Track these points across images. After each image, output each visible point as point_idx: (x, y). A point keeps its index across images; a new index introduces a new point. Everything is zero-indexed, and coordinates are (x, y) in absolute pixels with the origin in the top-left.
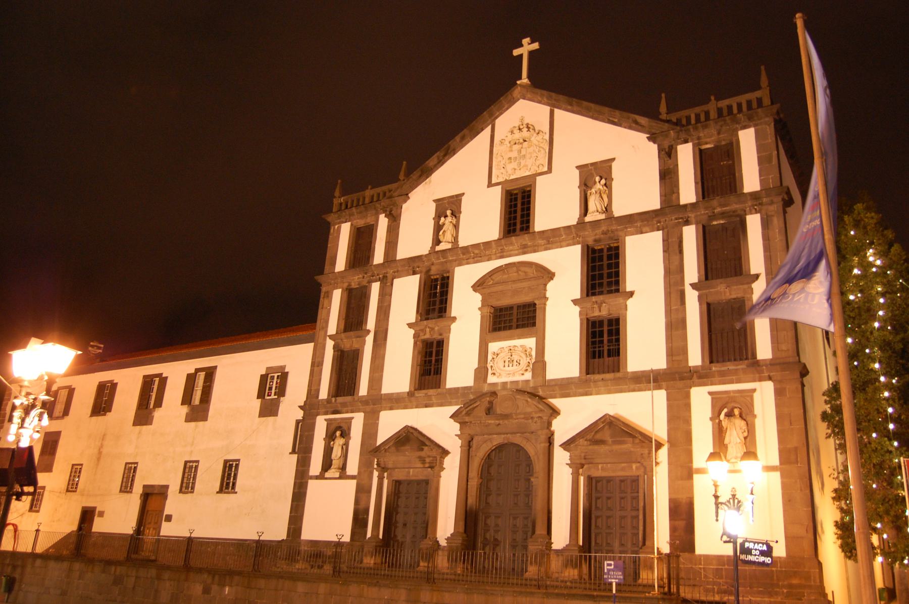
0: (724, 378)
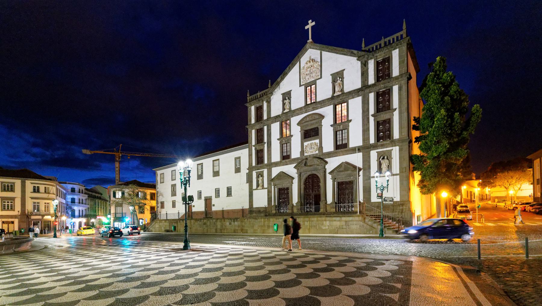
0: (383, 146)
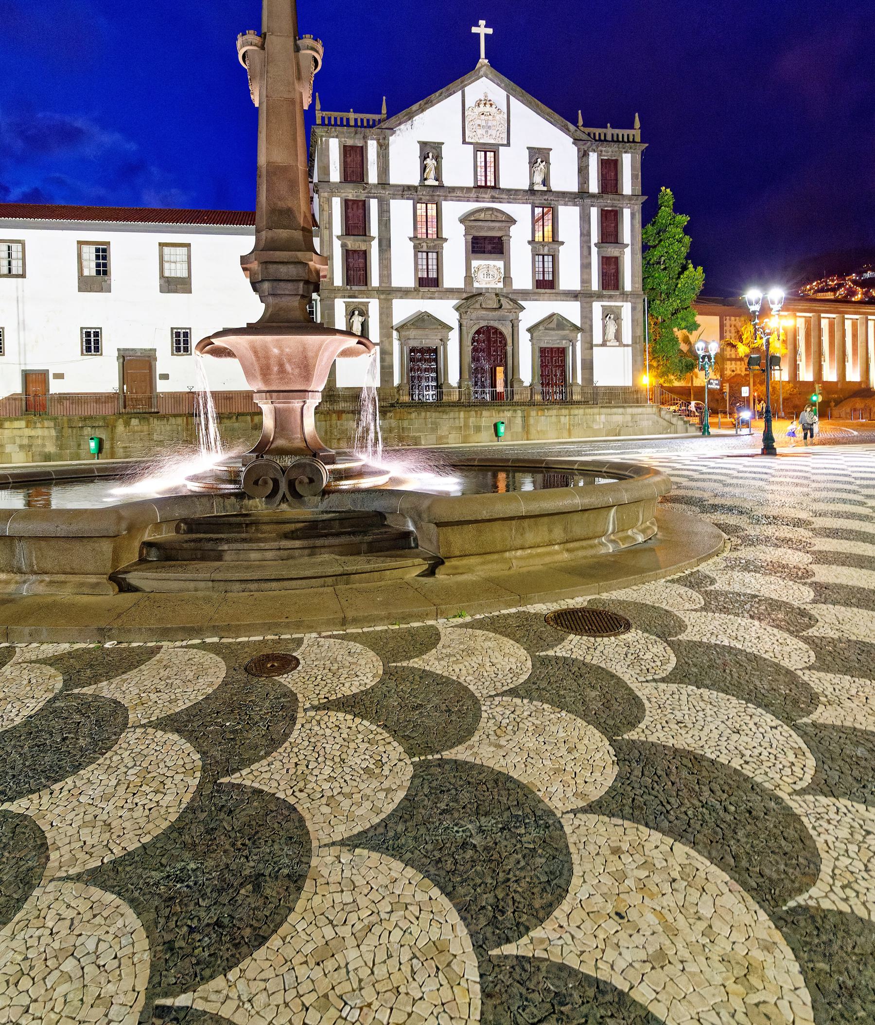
0: (610, 297)
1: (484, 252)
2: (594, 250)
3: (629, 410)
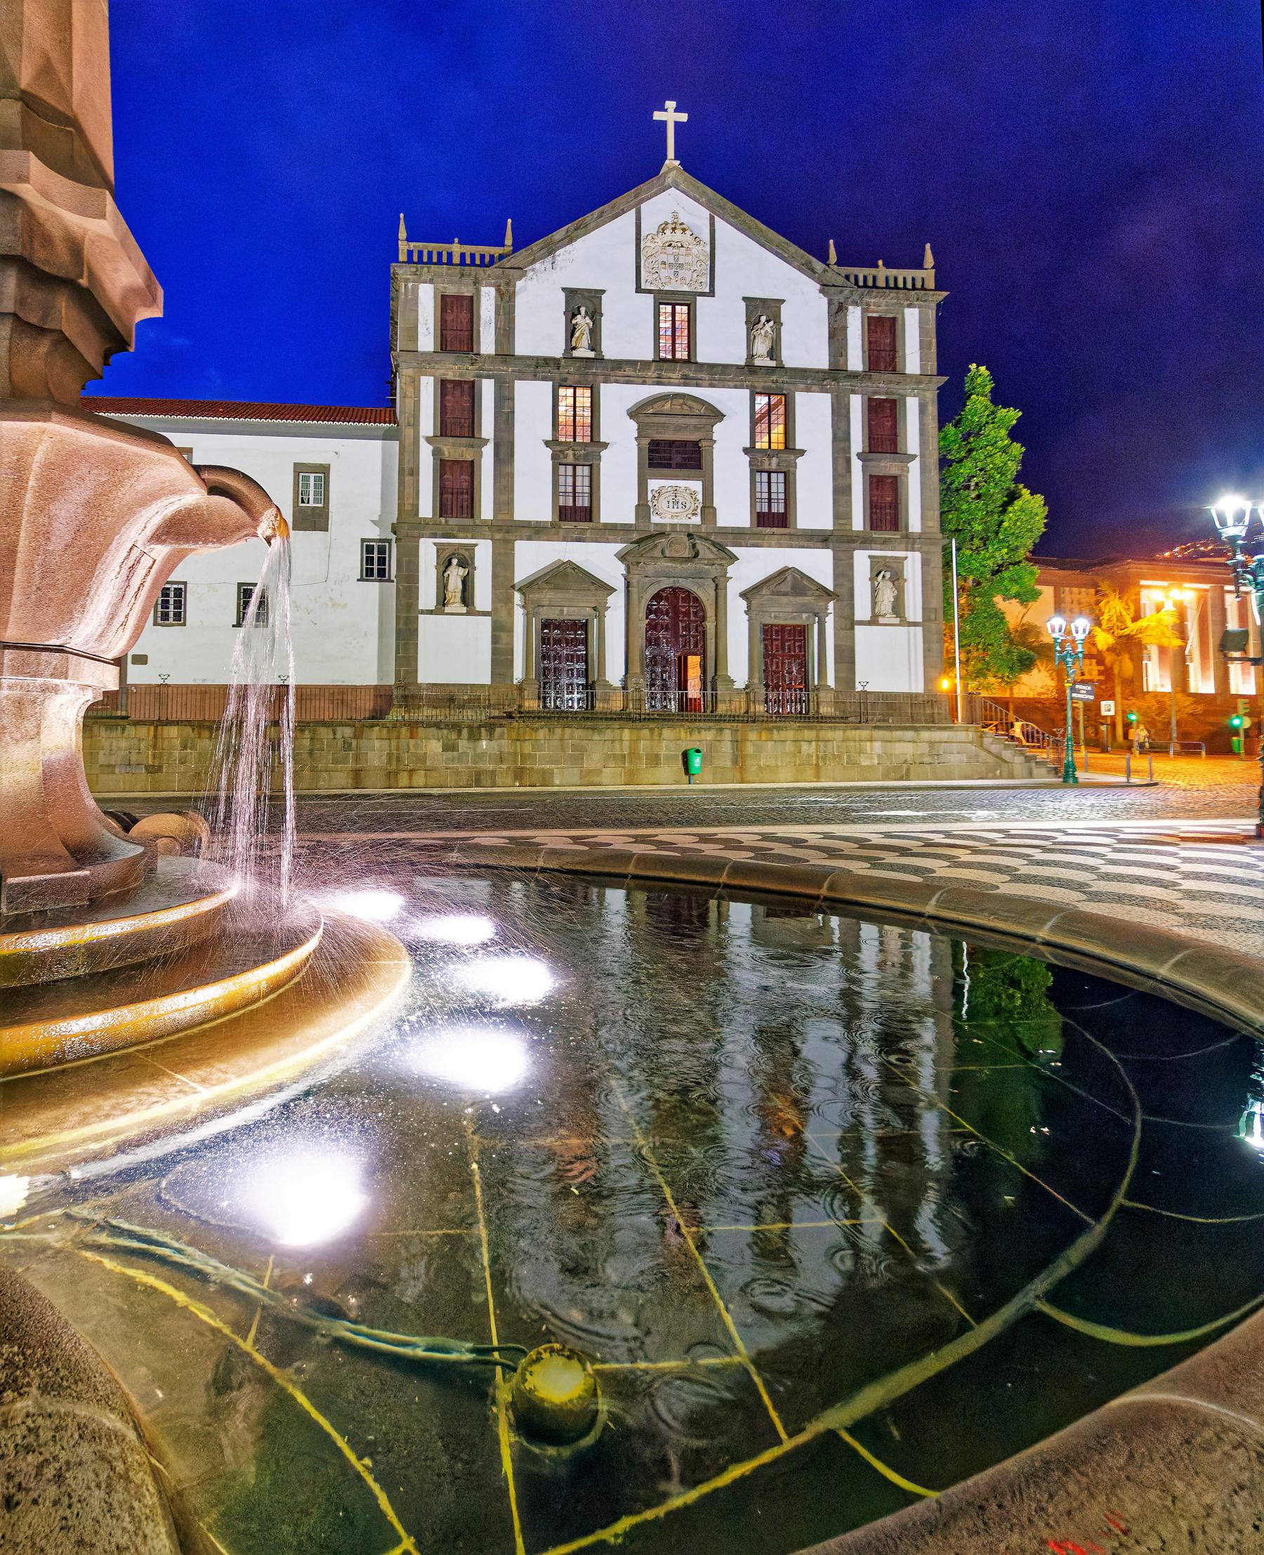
0: (885, 543)
1: (669, 466)
2: (857, 465)
3: (925, 735)
